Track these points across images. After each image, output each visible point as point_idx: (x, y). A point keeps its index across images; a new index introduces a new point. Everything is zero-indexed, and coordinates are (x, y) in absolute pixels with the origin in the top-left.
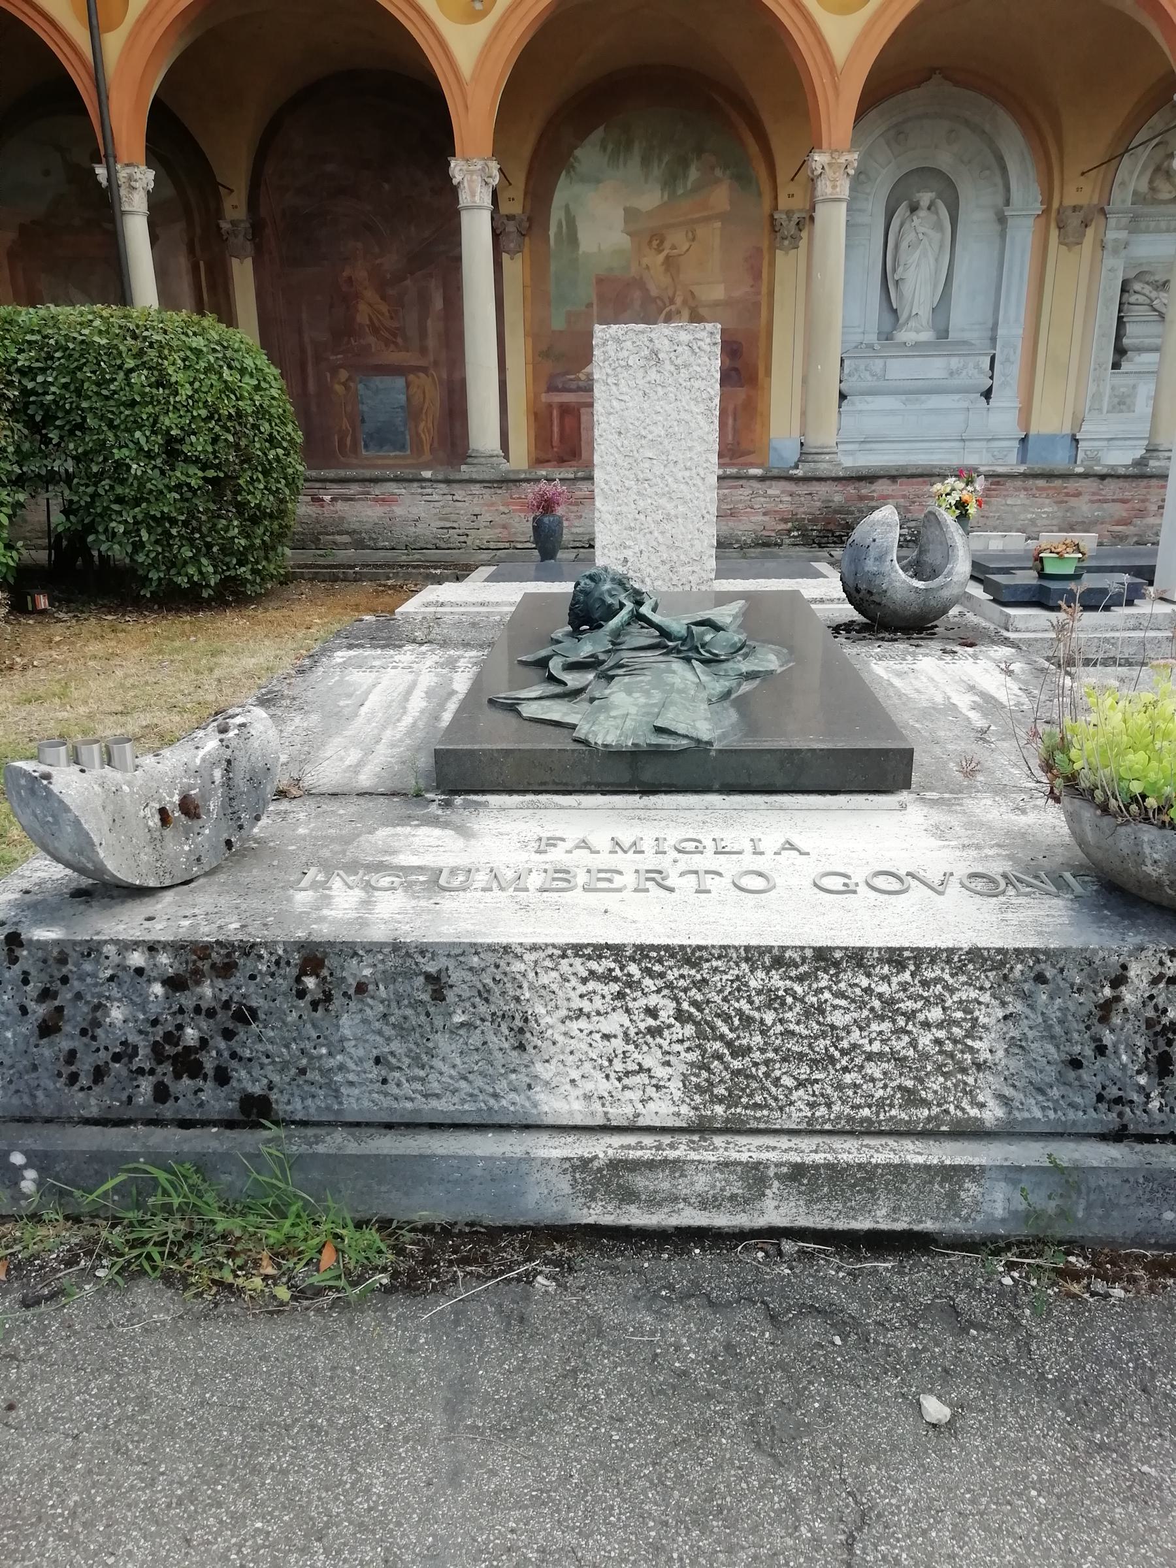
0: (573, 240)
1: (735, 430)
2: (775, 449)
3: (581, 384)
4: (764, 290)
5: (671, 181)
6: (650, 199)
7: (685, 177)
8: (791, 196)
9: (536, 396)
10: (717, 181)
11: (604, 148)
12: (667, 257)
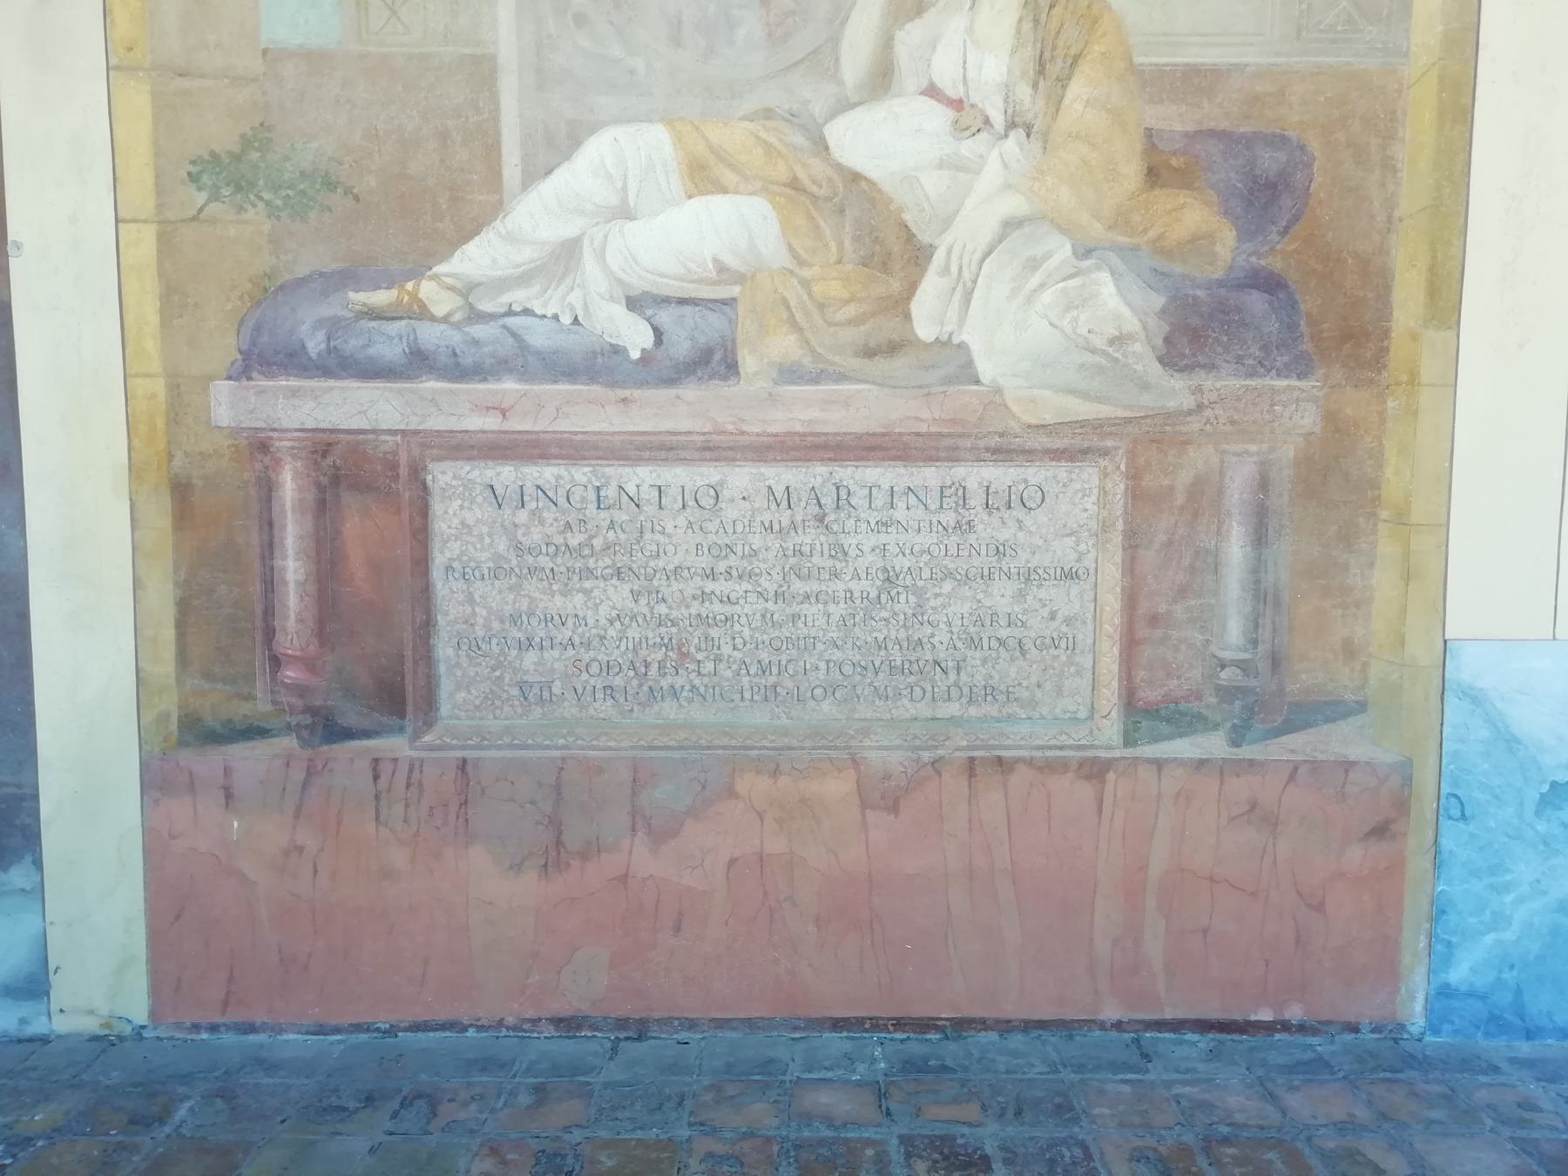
1: (1262, 596)
2: (1475, 698)
3: (430, 335)
9: (181, 399)
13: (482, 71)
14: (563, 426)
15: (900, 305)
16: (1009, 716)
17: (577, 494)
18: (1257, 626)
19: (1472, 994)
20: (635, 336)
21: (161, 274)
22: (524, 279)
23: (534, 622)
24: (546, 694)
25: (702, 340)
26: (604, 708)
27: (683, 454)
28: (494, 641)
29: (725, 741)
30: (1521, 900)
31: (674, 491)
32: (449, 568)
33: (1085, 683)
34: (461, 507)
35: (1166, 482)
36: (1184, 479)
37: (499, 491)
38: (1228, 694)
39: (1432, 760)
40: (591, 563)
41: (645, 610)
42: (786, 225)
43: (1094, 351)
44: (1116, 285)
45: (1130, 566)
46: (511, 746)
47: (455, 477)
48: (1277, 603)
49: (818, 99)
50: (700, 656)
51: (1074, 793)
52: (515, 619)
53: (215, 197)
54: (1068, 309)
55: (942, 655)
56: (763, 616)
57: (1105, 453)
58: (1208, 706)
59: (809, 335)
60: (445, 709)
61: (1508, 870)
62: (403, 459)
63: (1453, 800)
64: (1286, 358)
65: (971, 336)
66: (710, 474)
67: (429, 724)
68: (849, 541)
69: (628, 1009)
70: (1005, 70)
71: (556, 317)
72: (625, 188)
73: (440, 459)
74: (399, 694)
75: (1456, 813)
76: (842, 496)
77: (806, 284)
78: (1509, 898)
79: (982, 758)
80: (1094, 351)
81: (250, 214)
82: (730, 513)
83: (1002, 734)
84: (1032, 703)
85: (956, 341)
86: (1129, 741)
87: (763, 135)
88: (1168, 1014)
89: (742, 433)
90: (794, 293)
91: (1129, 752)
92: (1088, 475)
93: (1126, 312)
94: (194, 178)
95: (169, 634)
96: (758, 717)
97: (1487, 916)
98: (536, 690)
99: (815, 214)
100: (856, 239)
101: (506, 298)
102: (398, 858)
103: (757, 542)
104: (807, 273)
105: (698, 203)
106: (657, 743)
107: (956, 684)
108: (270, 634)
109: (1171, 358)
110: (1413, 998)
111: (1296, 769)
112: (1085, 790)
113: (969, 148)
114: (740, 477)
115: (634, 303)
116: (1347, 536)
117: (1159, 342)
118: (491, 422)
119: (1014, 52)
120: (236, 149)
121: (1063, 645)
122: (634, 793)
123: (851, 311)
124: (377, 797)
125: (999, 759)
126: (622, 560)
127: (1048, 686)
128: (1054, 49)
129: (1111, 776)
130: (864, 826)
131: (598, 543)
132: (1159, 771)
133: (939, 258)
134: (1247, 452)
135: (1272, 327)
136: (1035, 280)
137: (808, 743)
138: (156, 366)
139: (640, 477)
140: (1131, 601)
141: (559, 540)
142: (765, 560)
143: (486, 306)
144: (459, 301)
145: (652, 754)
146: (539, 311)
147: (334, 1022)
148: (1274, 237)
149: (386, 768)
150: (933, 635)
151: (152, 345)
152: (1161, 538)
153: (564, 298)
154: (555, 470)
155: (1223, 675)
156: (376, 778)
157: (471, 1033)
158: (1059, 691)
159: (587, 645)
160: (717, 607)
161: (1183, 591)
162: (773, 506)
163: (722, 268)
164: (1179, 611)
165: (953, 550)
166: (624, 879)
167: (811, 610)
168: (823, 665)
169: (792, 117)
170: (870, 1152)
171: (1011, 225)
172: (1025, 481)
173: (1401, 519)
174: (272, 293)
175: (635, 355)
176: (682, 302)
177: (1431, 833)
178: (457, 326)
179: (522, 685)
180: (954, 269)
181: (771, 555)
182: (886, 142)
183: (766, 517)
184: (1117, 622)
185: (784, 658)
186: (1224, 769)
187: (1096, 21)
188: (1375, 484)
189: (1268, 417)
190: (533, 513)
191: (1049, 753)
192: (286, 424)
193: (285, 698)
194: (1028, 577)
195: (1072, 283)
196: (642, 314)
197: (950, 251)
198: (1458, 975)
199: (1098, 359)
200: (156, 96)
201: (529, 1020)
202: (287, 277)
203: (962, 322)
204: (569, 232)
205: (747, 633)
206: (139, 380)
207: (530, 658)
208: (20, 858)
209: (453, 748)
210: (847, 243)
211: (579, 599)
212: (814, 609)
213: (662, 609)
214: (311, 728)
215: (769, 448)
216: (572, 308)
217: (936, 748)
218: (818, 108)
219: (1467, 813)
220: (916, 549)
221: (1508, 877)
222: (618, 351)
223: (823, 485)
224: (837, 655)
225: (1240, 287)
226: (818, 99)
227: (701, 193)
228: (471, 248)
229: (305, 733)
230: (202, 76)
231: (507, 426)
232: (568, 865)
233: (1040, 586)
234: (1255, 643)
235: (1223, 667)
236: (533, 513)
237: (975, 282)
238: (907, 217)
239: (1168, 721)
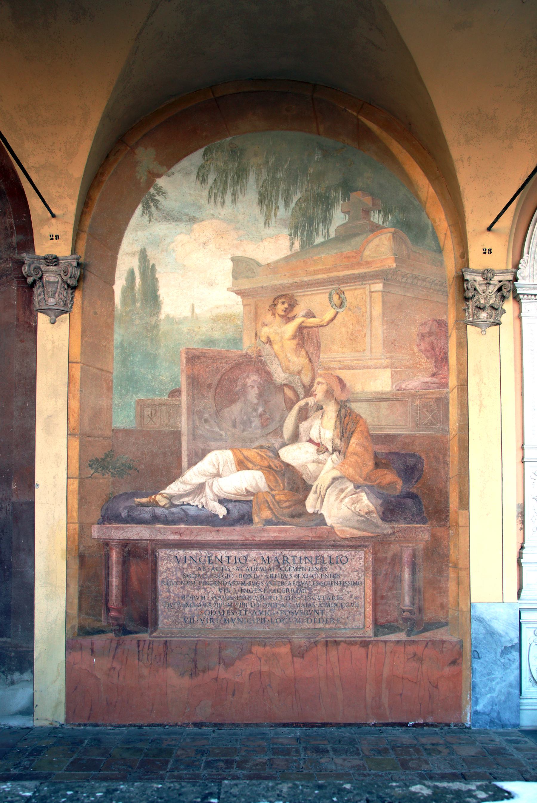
0: (151, 297)
1: (415, 590)
2: (481, 620)
3: (159, 511)
4: (453, 381)
5: (304, 226)
6: (273, 246)
7: (327, 221)
8: (487, 251)
9: (83, 530)
10: (375, 229)
11: (202, 178)
12: (301, 328)
13: (177, 435)
14: (199, 538)
15: (302, 502)
16: (338, 627)
17: (203, 558)
18: (414, 599)
19: (485, 713)
20: (221, 511)
21: (80, 493)
22: (187, 495)
23: (189, 598)
24: (192, 621)
25: (242, 512)
26: (210, 625)
27: (236, 547)
28: (176, 604)
29: (249, 635)
30: (498, 683)
31: (233, 558)
32: (163, 581)
33: (362, 617)
34: (167, 564)
35: (385, 555)
36: (390, 554)
37: (179, 558)
38: (406, 620)
39: (469, 640)
40: (207, 580)
41: (223, 595)
42: (267, 479)
43: (361, 516)
44: (368, 497)
45: (374, 581)
46: (181, 637)
47: (165, 554)
48: (420, 592)
49: (275, 442)
50: (240, 609)
51: (358, 651)
52: (183, 597)
53: (96, 471)
54: (353, 504)
55: (317, 609)
56: (261, 597)
57: (366, 546)
58: (400, 624)
59: (274, 511)
60: (160, 625)
61: (493, 674)
62: (150, 548)
63: (475, 653)
64: (419, 518)
65: (324, 511)
66: (244, 553)
67: (156, 630)
68: (287, 573)
69: (217, 720)
70: (332, 435)
71: (197, 506)
72: (218, 468)
73: (161, 548)
74: (146, 620)
75: (476, 656)
76: (285, 560)
77: (273, 496)
78: (494, 683)
79: (330, 641)
80: (361, 516)
81: (106, 476)
82: (250, 564)
83: (336, 633)
84: (345, 624)
85: (319, 513)
86: (375, 635)
87: (260, 453)
88: (390, 721)
89: (254, 540)
90: (269, 499)
91: (376, 638)
92: (361, 553)
93: (371, 505)
94: (90, 466)
95: (76, 601)
96: (260, 628)
97: (487, 689)
98: (189, 619)
99: (276, 476)
100: (288, 483)
101: (182, 500)
102: (145, 672)
103: (258, 573)
104: (274, 493)
105: (241, 472)
106: (227, 636)
107: (322, 618)
108: (107, 601)
109: (384, 518)
110: (466, 715)
111: (427, 643)
112: (363, 651)
113: (322, 457)
114: (253, 554)
115: (221, 501)
116: (440, 571)
117: (381, 513)
118: (177, 537)
119: (334, 430)
120: (103, 457)
121: (355, 605)
122: (220, 652)
123: (287, 504)
124: (139, 652)
125: (335, 641)
126: (216, 579)
127: (350, 618)
128: (346, 429)
129: (370, 646)
130: (293, 662)
131: (209, 574)
132: (385, 644)
133: (314, 488)
134: (408, 546)
135: (414, 509)
136: (343, 495)
137: (275, 636)
138: (76, 520)
139: (222, 554)
140: (375, 591)
141: (197, 573)
142: (261, 579)
143: (176, 503)
144: (168, 501)
145: (226, 639)
146: (192, 504)
147: (123, 723)
148: (414, 483)
149: (142, 644)
150: (314, 602)
151: (75, 514)
152: (384, 572)
153: (200, 500)
154: (196, 552)
155: (404, 614)
156: (139, 646)
157: (167, 727)
158: (354, 620)
159: (205, 605)
160: (246, 594)
161: (391, 589)
162: (264, 563)
163: (247, 491)
164: (390, 594)
165: (320, 576)
166: (216, 679)
167: (276, 595)
168: (279, 612)
169: (269, 448)
170: (294, 749)
171: (335, 479)
172: (342, 555)
173: (456, 566)
174: (112, 499)
175: (221, 517)
176: (236, 501)
177: (469, 663)
178: (167, 508)
179: (185, 618)
180: (318, 492)
181: (263, 578)
182: (297, 455)
183: (262, 566)
184: (371, 598)
185: (267, 609)
186: (405, 643)
187: (358, 421)
188: (448, 556)
189: (415, 536)
190: (189, 564)
191: (351, 639)
192: (114, 538)
193: (111, 621)
194: (343, 584)
195: (354, 496)
196: (223, 505)
197: (317, 487)
198: (479, 708)
199: (362, 518)
200: (80, 442)
201: (186, 723)
202: (117, 494)
203: (321, 507)
204: (202, 480)
205: (255, 602)
206: (71, 524)
207: (187, 609)
209: (162, 637)
210: (286, 484)
211: (203, 591)
212: (277, 594)
213: (229, 594)
214: (119, 630)
215: (262, 545)
216: (202, 503)
217: (316, 637)
218: (276, 446)
219: (480, 656)
220: (309, 576)
221: (493, 676)
222: (216, 516)
223: (279, 556)
224: (284, 609)
225: (404, 497)
226: (275, 442)
227: (242, 470)
228: (172, 486)
229: (117, 632)
230: (95, 437)
231: (181, 538)
232: (199, 674)
233: (347, 587)
234: (413, 604)
235: (404, 612)
236: (189, 564)
237: (325, 496)
238: (304, 477)
239: (388, 628)
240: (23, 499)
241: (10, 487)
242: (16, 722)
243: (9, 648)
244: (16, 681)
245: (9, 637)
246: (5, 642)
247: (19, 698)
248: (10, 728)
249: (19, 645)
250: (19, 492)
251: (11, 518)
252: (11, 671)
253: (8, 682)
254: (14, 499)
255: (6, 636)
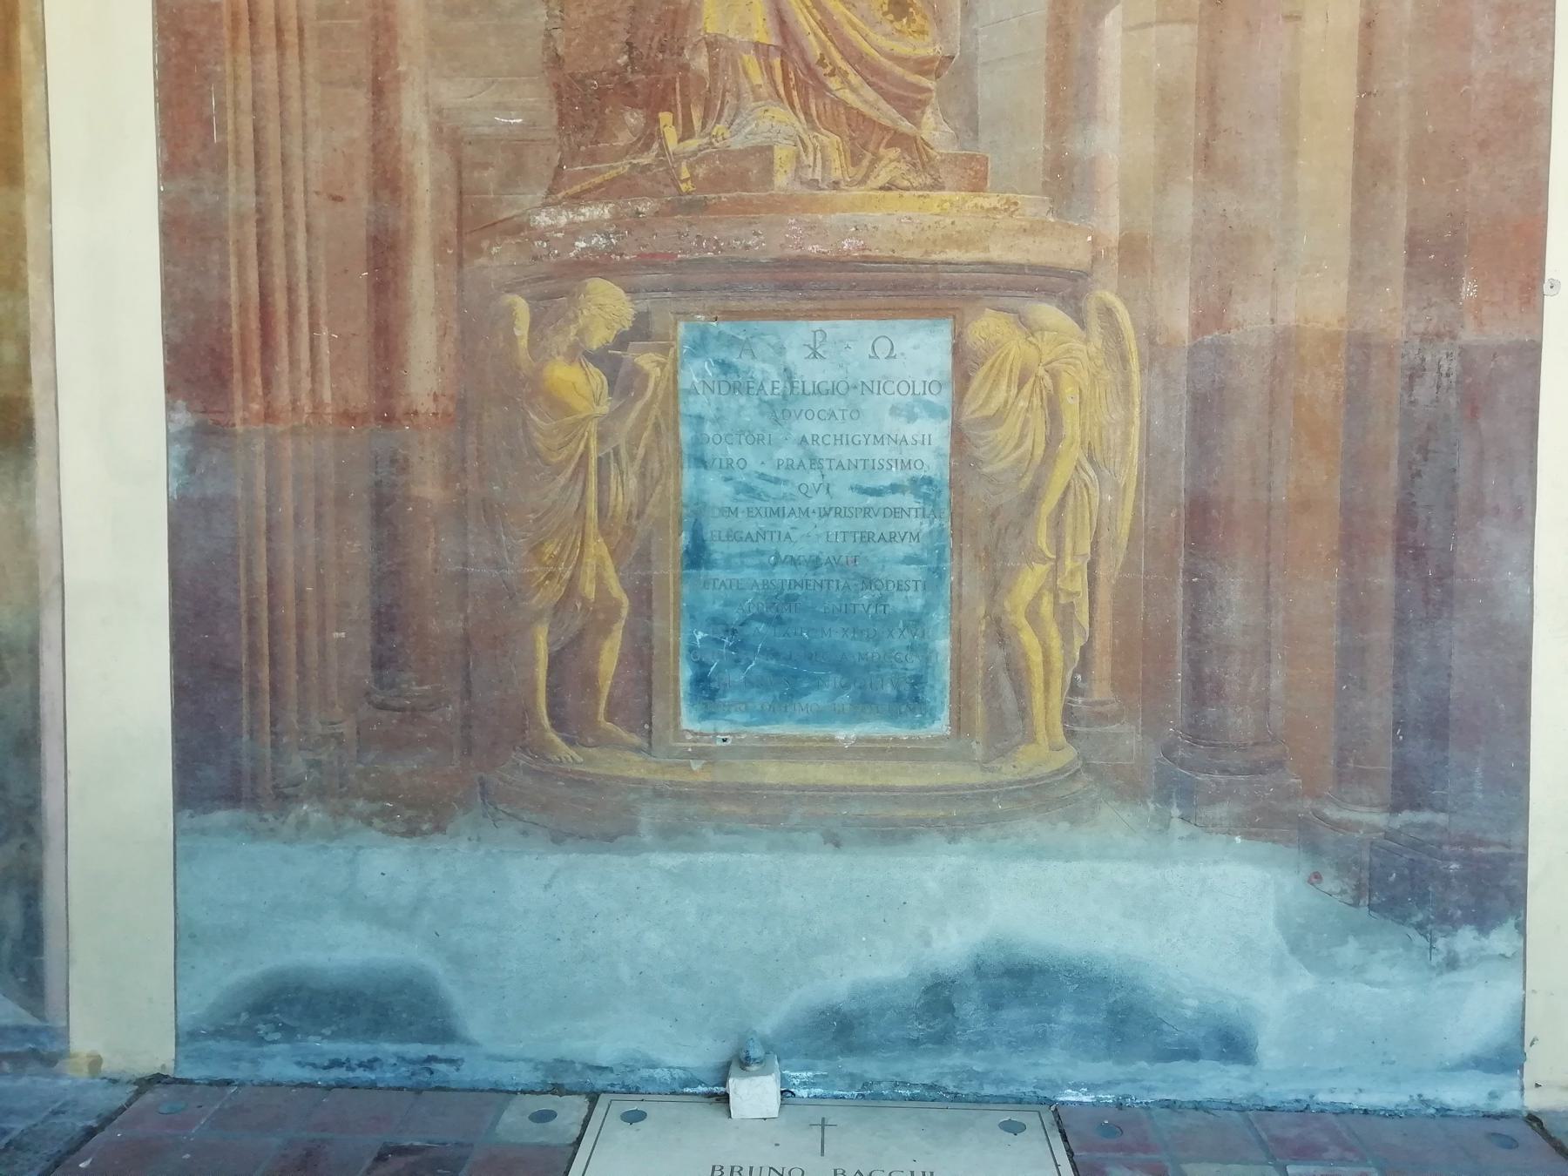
208: (1499, 920)
240: (1499, 332)
241: (1453, 291)
242: (1464, 1094)
243: (1440, 846)
244: (1462, 957)
245: (1443, 811)
246: (1427, 827)
247: (1473, 1011)
248: (1444, 1112)
249: (1478, 835)
250: (1486, 310)
251: (1453, 401)
252: (1447, 921)
253: (1437, 959)
254: (1468, 335)
255: (1432, 807)
